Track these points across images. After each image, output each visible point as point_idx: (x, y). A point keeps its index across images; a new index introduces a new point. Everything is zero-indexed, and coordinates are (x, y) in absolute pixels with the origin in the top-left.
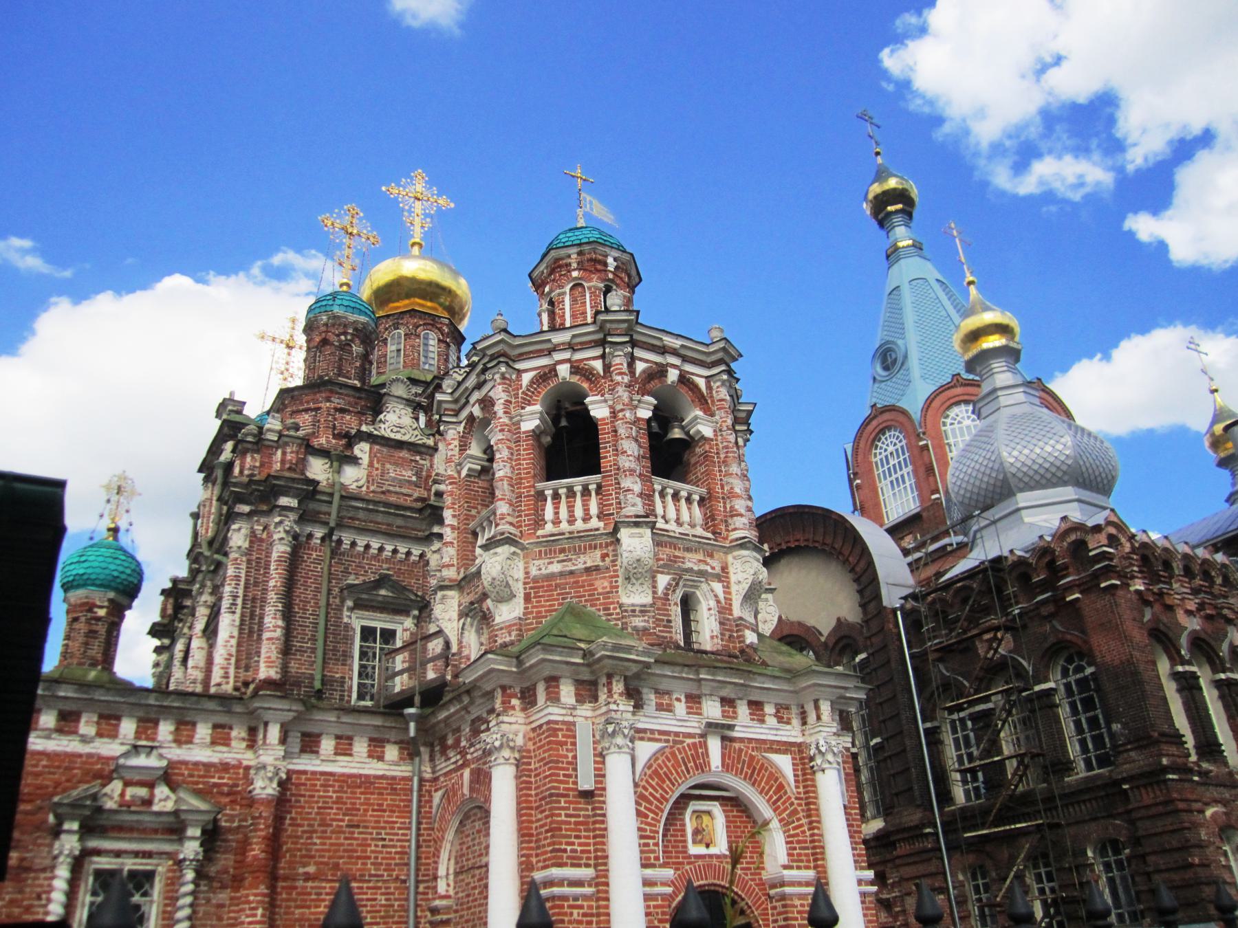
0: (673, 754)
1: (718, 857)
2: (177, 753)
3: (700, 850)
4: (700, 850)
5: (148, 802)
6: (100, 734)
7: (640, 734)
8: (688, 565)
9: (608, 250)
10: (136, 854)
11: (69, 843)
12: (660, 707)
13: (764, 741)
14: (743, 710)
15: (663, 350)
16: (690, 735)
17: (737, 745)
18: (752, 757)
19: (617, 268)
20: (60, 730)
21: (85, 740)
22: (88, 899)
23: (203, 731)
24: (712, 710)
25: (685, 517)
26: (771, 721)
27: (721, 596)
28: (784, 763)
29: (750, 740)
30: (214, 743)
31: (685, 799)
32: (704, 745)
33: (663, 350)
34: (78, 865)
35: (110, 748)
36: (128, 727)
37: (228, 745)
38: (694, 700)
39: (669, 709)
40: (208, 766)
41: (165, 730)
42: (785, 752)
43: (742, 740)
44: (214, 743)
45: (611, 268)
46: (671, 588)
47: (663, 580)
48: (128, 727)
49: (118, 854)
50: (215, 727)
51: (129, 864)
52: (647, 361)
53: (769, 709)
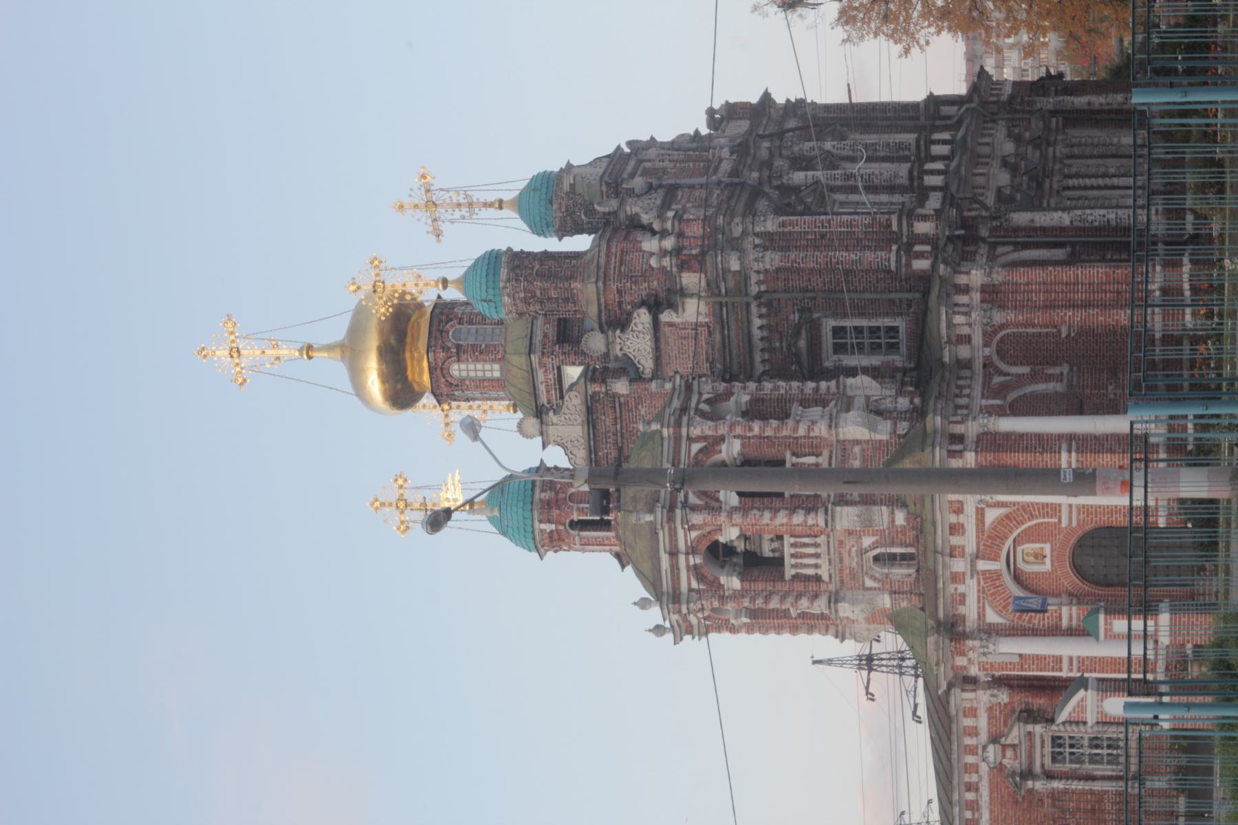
0: (992, 595)
1: (1052, 550)
2: (984, 736)
3: (1048, 560)
4: (1048, 560)
5: (1014, 746)
6: (977, 772)
7: (981, 615)
8: (854, 564)
9: (537, 532)
10: (1043, 747)
11: (1039, 785)
12: (963, 602)
13: (977, 526)
14: (955, 540)
15: (674, 568)
16: (979, 582)
17: (982, 548)
18: (989, 537)
19: (549, 521)
20: (977, 790)
21: (981, 778)
22: (1068, 765)
23: (968, 722)
24: (959, 565)
25: (811, 550)
26: (962, 519)
27: (873, 539)
28: (991, 515)
29: (978, 537)
30: (975, 716)
31: (1018, 578)
32: (984, 572)
33: (674, 568)
34: (1050, 776)
35: (984, 768)
36: (970, 759)
37: (976, 709)
38: (956, 578)
39: (963, 596)
40: (990, 718)
41: (969, 741)
42: (983, 515)
43: (978, 544)
44: (975, 716)
45: (553, 527)
46: (873, 578)
47: (869, 583)
48: (970, 759)
49: (1043, 756)
50: (965, 716)
51: (1048, 749)
52: (689, 579)
53: (953, 519)
